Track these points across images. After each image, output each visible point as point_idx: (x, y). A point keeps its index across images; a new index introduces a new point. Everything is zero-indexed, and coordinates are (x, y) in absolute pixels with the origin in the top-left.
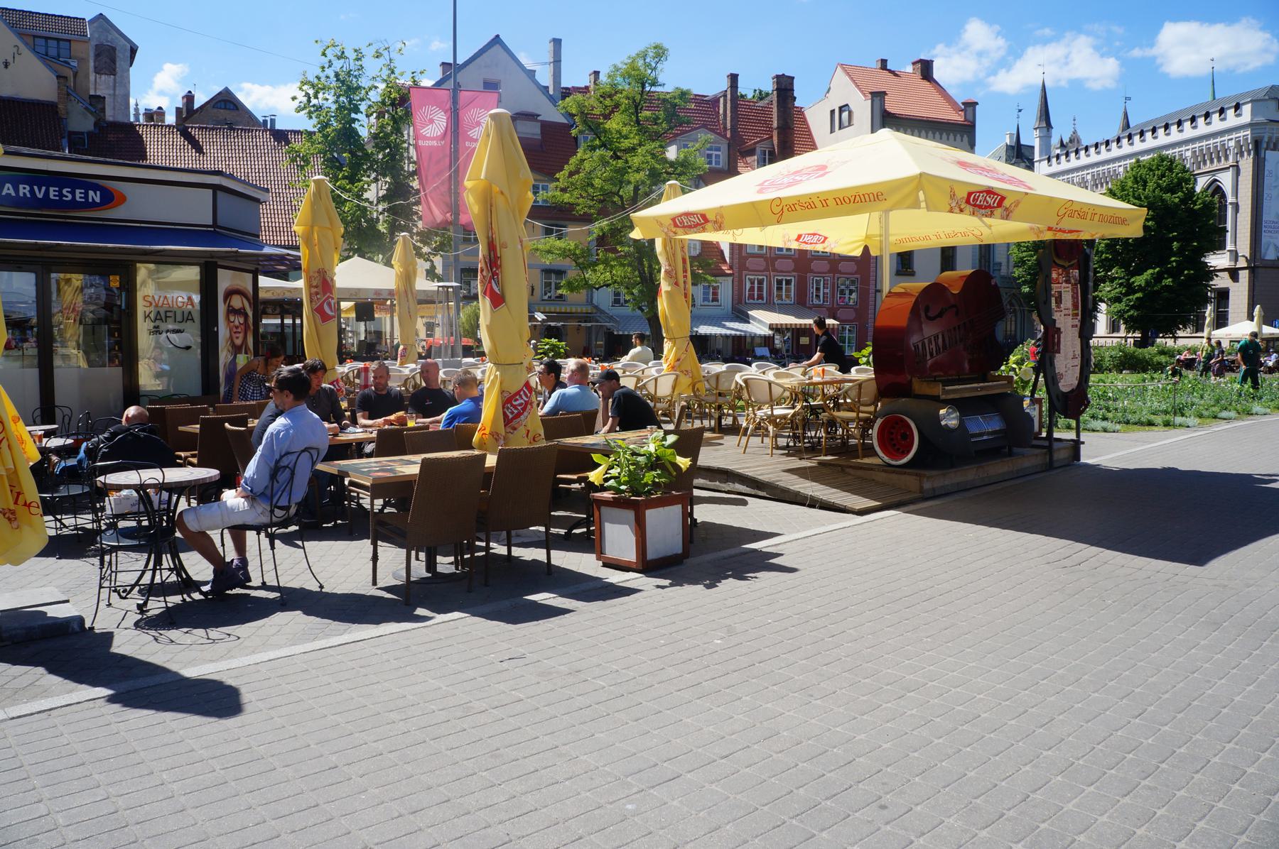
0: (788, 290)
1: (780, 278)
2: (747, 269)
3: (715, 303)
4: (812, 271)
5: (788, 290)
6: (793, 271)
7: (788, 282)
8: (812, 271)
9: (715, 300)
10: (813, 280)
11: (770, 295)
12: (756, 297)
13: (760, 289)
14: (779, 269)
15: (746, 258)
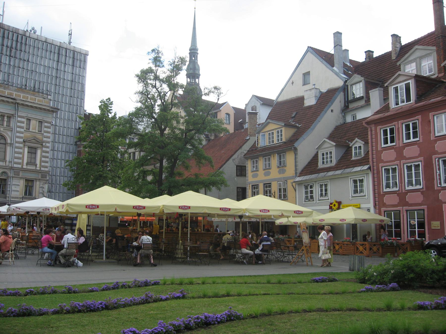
0: (417, 175)
1: (409, 165)
2: (383, 161)
3: (362, 194)
4: (436, 153)
5: (417, 175)
6: (420, 156)
7: (417, 167)
8: (436, 153)
9: (362, 191)
10: (438, 161)
11: (401, 183)
12: (414, 183)
13: (410, 176)
14: (407, 157)
15: (381, 152)
